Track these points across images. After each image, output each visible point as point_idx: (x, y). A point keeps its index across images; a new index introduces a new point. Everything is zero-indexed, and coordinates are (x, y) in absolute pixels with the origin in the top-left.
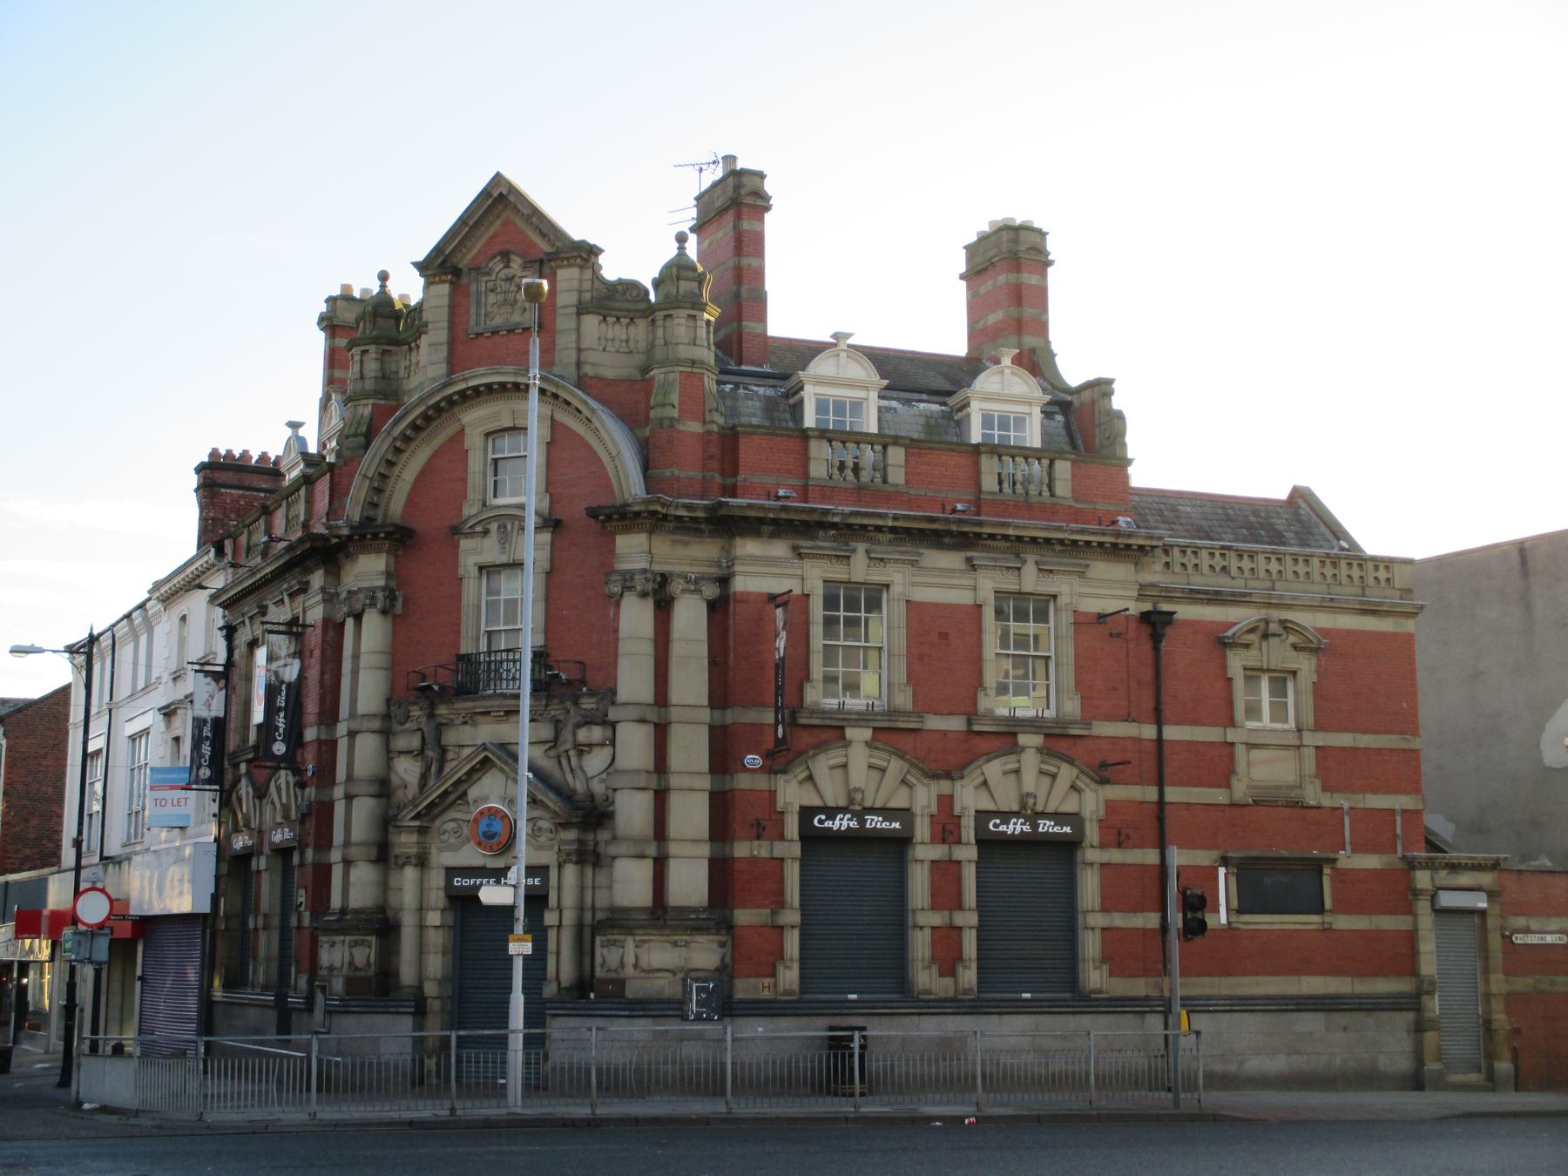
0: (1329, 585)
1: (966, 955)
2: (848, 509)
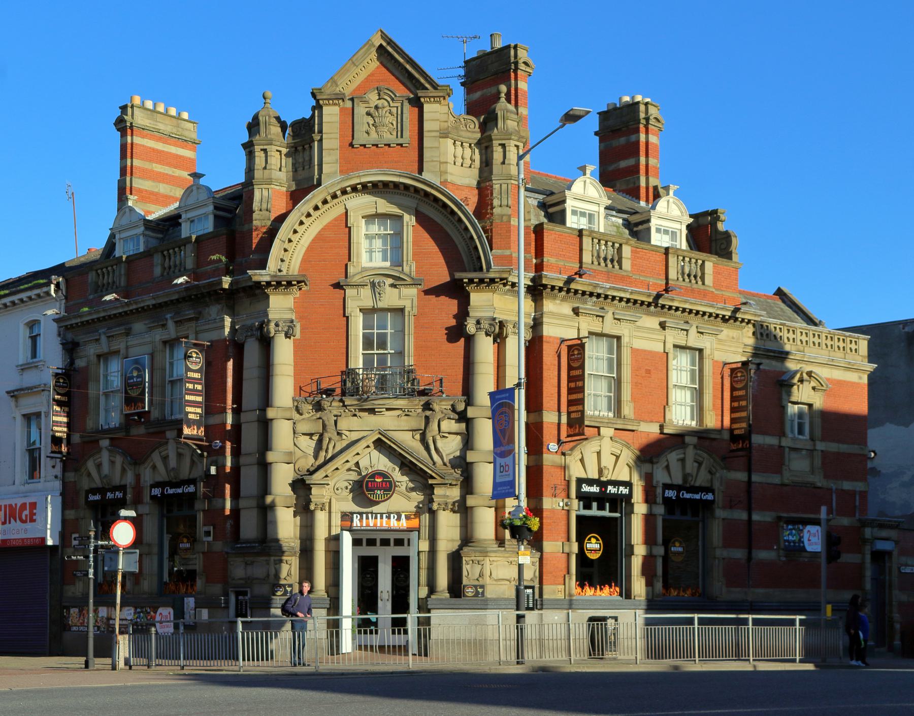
0: (829, 351)
1: (658, 574)
2: (608, 285)
